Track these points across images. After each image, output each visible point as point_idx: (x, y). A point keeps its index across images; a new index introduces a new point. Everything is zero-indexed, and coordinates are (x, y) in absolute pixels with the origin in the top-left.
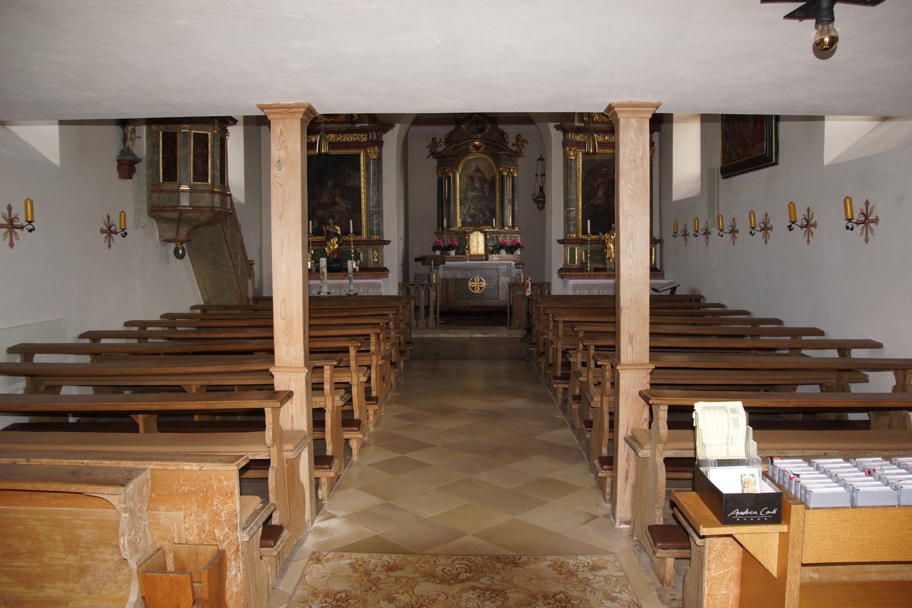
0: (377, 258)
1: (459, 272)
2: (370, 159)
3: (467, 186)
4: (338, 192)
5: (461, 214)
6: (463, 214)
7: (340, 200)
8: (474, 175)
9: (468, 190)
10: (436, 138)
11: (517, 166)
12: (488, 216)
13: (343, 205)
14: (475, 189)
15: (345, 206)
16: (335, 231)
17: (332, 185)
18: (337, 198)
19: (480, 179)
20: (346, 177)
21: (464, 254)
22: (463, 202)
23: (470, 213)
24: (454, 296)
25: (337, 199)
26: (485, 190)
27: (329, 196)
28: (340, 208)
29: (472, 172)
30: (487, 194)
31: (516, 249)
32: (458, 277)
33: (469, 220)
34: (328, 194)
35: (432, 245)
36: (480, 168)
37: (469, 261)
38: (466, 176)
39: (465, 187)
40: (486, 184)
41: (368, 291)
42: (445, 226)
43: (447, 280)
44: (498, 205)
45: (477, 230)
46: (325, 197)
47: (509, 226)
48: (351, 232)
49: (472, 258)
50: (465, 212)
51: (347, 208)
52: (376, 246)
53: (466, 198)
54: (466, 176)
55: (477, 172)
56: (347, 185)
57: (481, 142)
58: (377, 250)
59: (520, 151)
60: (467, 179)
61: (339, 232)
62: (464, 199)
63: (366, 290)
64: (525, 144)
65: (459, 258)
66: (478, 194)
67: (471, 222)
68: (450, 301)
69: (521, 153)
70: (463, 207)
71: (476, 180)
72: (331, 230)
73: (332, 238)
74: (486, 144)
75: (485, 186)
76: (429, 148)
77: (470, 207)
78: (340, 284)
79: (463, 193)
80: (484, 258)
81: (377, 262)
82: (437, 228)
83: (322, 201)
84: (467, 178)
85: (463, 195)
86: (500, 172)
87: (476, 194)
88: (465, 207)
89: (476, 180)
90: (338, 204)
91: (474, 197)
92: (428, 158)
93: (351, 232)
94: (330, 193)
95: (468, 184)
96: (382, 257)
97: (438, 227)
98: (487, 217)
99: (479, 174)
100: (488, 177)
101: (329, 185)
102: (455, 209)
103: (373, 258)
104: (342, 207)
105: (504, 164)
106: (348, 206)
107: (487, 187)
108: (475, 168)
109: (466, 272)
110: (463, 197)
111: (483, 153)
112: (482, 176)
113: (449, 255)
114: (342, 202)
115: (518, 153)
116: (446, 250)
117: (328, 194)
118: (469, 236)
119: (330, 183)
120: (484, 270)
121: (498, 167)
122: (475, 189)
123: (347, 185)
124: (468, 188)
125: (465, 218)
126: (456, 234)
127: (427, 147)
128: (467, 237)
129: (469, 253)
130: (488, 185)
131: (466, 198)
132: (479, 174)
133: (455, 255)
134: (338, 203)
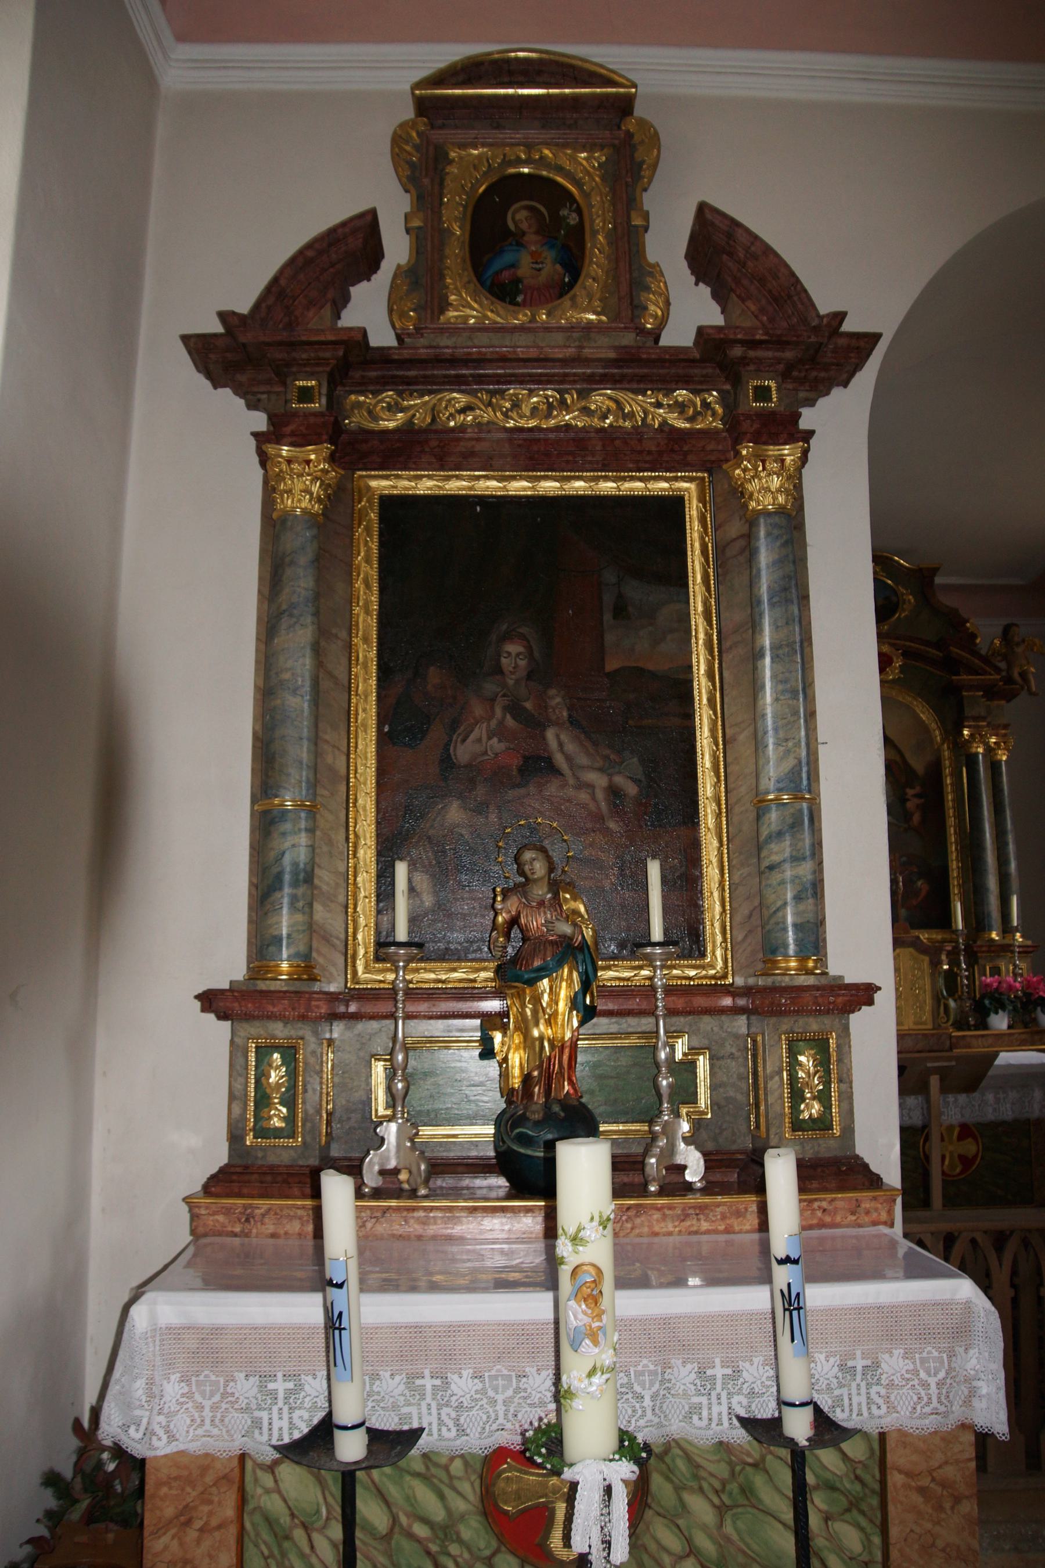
0: (823, 1098)
2: (752, 521)
4: (556, 699)
7: (570, 747)
13: (592, 777)
15: (599, 780)
16: (567, 929)
17: (522, 663)
18: (550, 734)
20: (608, 617)
25: (553, 744)
27: (510, 721)
28: (571, 792)
34: (498, 712)
41: (876, 1365)
46: (480, 731)
48: (657, 934)
51: (614, 792)
52: (814, 1025)
56: (612, 665)
57: (892, 645)
58: (820, 1046)
61: (588, 933)
63: (859, 1363)
72: (536, 922)
73: (543, 972)
74: (906, 654)
78: (666, 1322)
81: (822, 1124)
83: (463, 753)
90: (555, 771)
93: (657, 934)
94: (515, 709)
96: (847, 1097)
101: (504, 661)
103: (797, 1096)
104: (581, 785)
106: (619, 780)
114: (583, 760)
117: (498, 712)
119: (513, 648)
123: (612, 665)
134: (559, 760)
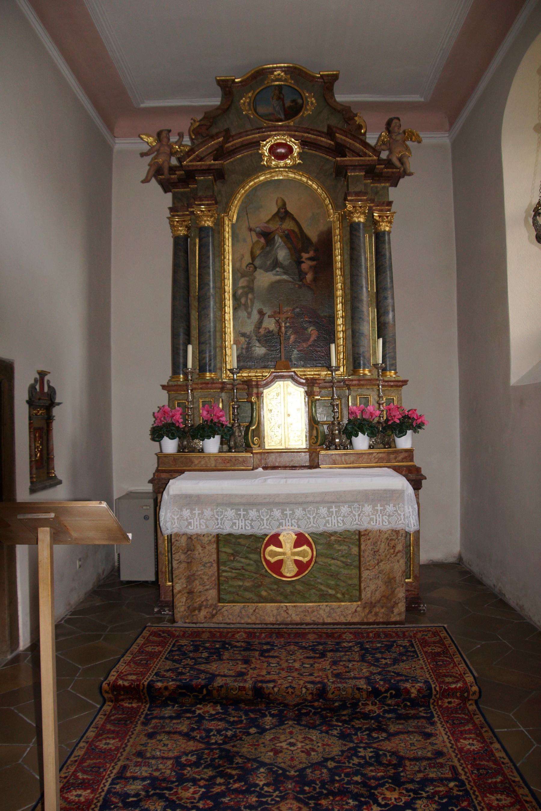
1: (230, 513)
3: (253, 258)
5: (239, 334)
6: (244, 335)
8: (272, 227)
9: (256, 268)
10: (170, 131)
11: (390, 204)
12: (313, 337)
14: (276, 264)
19: (288, 237)
21: (248, 448)
22: (243, 300)
23: (262, 331)
24: (213, 593)
26: (304, 266)
29: (270, 217)
30: (309, 277)
31: (402, 433)
32: (227, 529)
33: (260, 350)
35: (150, 422)
36: (289, 209)
37: (260, 469)
38: (251, 230)
39: (247, 259)
40: (308, 253)
42: (190, 365)
43: (190, 538)
44: (339, 306)
45: (282, 377)
47: (376, 365)
49: (271, 460)
50: (249, 329)
53: (250, 289)
54: (251, 230)
55: (283, 219)
59: (400, 160)
60: (255, 238)
62: (246, 294)
64: (409, 143)
65: (230, 460)
66: (285, 277)
67: (265, 355)
68: (200, 610)
69: (402, 163)
70: (243, 314)
71: (279, 241)
75: (305, 256)
76: (151, 157)
77: (261, 313)
79: (243, 276)
80: (305, 458)
82: (169, 373)
84: (253, 233)
85: (243, 282)
86: (345, 217)
87: (278, 278)
88: (249, 315)
89: (279, 241)
91: (274, 286)
92: (146, 181)
95: (258, 252)
97: (175, 372)
98: (310, 343)
99: (288, 225)
100: (313, 234)
102: (222, 320)
105: (357, 194)
107: (310, 259)
108: (275, 210)
109: (253, 513)
110: (243, 287)
111: (294, 168)
112: (297, 230)
113: (202, 451)
115: (395, 167)
116: (194, 437)
118: (259, 396)
120: (311, 508)
121: (339, 205)
122: (276, 264)
124: (257, 262)
125: (249, 348)
126: (222, 389)
127: (143, 155)
128: (254, 399)
129: (261, 444)
130: (311, 254)
131: (250, 289)
132: (288, 225)
133: (221, 451)
